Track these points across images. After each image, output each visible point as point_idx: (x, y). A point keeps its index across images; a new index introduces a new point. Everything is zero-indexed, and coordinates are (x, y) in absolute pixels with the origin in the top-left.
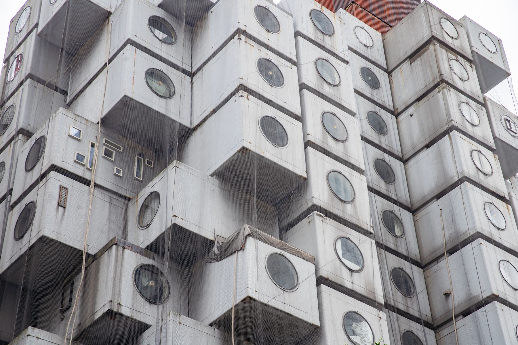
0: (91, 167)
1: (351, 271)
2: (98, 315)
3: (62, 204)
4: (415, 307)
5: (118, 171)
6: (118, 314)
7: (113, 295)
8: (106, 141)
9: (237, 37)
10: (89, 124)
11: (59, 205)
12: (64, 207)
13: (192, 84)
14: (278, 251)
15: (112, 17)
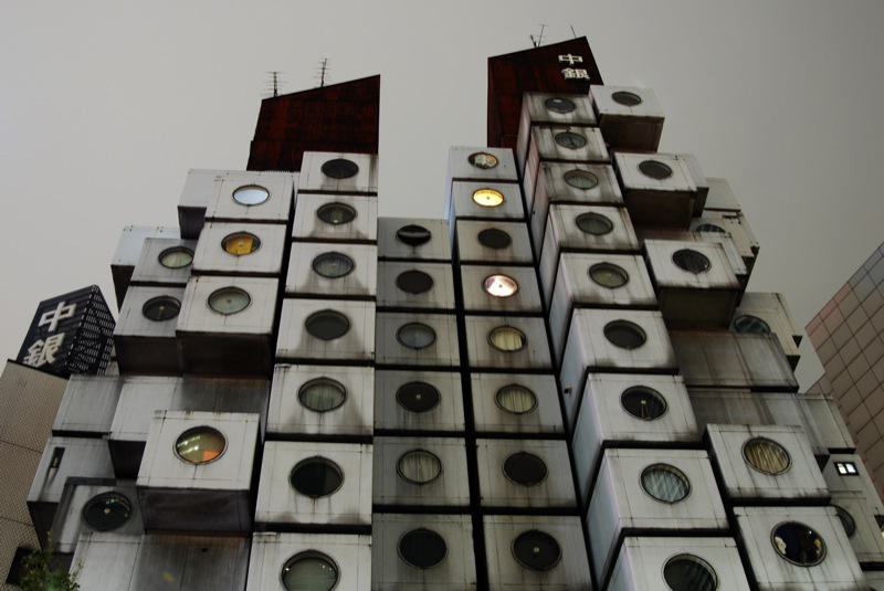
11: (51, 466)
12: (57, 467)
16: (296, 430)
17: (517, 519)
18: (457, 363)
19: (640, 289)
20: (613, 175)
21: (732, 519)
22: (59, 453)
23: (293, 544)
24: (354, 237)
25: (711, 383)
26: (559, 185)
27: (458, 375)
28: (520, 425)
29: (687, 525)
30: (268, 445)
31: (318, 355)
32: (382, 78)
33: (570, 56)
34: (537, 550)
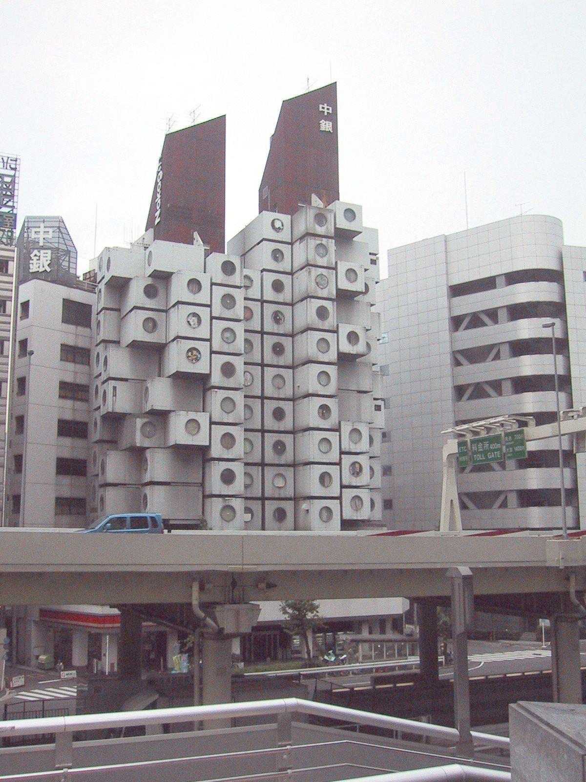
3: (115, 395)
11: (113, 396)
12: (115, 396)
19: (332, 356)
21: (341, 459)
22: (115, 388)
23: (224, 466)
24: (235, 317)
26: (313, 284)
27: (260, 367)
29: (328, 461)
32: (227, 117)
33: (325, 106)
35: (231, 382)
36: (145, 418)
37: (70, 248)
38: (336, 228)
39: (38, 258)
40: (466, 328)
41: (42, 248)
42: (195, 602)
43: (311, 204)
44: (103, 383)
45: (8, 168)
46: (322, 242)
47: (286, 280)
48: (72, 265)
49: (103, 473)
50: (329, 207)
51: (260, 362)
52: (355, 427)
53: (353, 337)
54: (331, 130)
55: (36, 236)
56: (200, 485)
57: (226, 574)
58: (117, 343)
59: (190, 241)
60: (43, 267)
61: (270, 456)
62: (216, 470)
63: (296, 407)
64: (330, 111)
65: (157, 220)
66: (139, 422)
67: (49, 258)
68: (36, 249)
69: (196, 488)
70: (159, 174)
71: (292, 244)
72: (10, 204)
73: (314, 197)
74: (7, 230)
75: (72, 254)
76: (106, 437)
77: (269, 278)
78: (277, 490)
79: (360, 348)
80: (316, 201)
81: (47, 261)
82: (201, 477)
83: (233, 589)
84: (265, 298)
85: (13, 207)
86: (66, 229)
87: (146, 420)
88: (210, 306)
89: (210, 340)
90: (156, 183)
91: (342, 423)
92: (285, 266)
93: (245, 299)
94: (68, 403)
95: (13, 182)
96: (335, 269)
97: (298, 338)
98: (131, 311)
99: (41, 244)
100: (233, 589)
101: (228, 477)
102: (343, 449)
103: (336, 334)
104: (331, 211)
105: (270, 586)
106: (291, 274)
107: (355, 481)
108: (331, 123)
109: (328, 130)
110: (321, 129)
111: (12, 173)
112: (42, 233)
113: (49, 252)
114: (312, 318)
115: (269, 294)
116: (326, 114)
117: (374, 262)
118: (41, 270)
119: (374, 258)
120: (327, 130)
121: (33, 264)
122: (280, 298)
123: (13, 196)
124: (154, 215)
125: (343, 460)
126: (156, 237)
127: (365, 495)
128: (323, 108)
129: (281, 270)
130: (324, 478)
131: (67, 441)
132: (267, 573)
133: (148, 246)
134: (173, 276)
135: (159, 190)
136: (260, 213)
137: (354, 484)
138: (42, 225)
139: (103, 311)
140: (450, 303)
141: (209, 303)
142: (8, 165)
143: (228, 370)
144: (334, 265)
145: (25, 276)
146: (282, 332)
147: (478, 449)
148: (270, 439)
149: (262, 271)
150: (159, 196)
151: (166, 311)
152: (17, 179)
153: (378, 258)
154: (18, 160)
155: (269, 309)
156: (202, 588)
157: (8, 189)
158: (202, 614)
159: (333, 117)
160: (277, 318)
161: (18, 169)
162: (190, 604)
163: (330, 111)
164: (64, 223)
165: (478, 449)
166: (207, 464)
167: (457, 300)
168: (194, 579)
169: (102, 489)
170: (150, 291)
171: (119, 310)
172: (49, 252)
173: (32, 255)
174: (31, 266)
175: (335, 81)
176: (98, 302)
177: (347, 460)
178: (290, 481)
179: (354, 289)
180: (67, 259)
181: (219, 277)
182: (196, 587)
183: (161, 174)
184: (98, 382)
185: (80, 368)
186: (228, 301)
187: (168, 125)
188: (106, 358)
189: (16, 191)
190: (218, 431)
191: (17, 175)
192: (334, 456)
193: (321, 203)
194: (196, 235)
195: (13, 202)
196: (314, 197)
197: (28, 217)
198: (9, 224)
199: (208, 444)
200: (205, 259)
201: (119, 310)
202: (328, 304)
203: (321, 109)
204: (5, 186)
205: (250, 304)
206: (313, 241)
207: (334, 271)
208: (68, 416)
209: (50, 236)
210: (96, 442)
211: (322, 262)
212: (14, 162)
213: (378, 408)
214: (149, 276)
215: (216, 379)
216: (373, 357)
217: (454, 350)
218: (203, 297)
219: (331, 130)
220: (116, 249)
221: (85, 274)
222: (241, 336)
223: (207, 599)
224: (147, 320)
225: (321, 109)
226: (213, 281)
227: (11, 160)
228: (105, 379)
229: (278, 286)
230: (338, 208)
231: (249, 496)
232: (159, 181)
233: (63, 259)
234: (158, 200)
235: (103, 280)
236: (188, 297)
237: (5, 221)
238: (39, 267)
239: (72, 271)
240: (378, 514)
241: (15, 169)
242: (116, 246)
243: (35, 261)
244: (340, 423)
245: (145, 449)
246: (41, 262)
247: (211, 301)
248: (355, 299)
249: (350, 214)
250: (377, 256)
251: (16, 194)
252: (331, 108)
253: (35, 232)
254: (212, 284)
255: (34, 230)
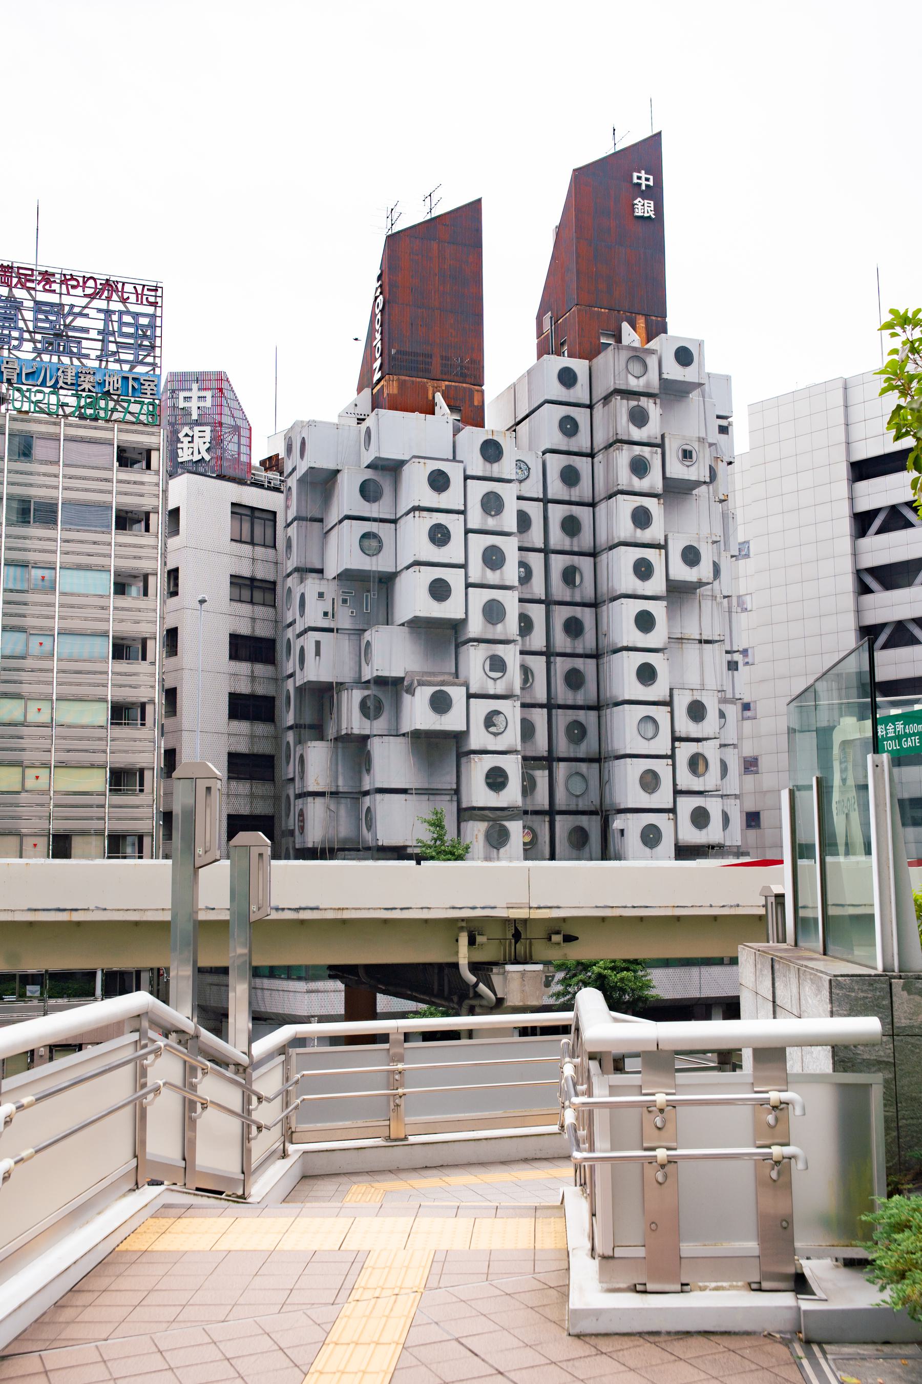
0: (333, 617)
1: (495, 680)
2: (343, 733)
3: (318, 653)
4: (581, 646)
5: (352, 612)
6: (352, 734)
7: (347, 725)
8: (343, 592)
9: (412, 515)
10: (330, 582)
11: (316, 655)
13: (396, 530)
14: (438, 688)
15: (339, 476)
16: (484, 692)
17: (570, 712)
18: (543, 598)
19: (656, 585)
20: (659, 456)
21: (673, 749)
22: (318, 644)
23: (489, 762)
25: (679, 636)
28: (574, 648)
30: (472, 700)
31: (489, 636)
33: (643, 174)
34: (576, 732)
35: (498, 631)
36: (367, 688)
37: (239, 423)
38: (660, 379)
39: (190, 439)
40: (880, 531)
41: (197, 423)
42: (463, 962)
43: (619, 340)
44: (300, 635)
45: (145, 302)
46: (640, 403)
47: (582, 464)
48: (244, 449)
49: (302, 778)
50: (652, 345)
51: (543, 598)
52: (695, 698)
53: (691, 556)
54: (652, 214)
55: (187, 405)
56: (453, 792)
57: (506, 921)
58: (321, 571)
59: (430, 410)
60: (199, 453)
61: (563, 747)
62: (479, 768)
63: (601, 667)
64: (651, 183)
65: (377, 376)
66: (357, 695)
67: (208, 439)
68: (186, 424)
69: (448, 798)
70: (378, 300)
71: (590, 407)
72: (149, 360)
73: (625, 326)
74: (146, 401)
75: (244, 433)
76: (308, 719)
77: (556, 463)
78: (574, 799)
79: (703, 571)
80: (631, 336)
81: (205, 443)
82: (455, 780)
83: (516, 943)
84: (550, 496)
85: (154, 365)
86: (233, 391)
87: (367, 692)
88: (463, 512)
89: (464, 566)
90: (373, 315)
91: (675, 692)
92: (582, 441)
93: (520, 498)
94: (244, 667)
95: (152, 326)
96: (662, 446)
97: (603, 557)
98: (340, 522)
99: (195, 416)
100: (516, 943)
101: (496, 780)
102: (677, 734)
103: (663, 551)
104: (652, 352)
105: (569, 939)
106: (592, 455)
107: (696, 784)
108: (652, 202)
109: (648, 215)
110: (636, 214)
111: (150, 310)
112: (195, 399)
113: (208, 429)
114: (625, 528)
115: (556, 488)
116: (643, 188)
117: (724, 430)
118: (196, 457)
119: (724, 423)
120: (646, 215)
121: (182, 449)
122: (575, 494)
123: (153, 347)
124: (372, 367)
125: (677, 750)
126: (376, 404)
127: (714, 807)
128: (639, 178)
129: (575, 449)
130: (650, 781)
131: (243, 727)
132: (564, 920)
133: (362, 417)
134: (406, 468)
135: (378, 327)
136: (538, 359)
137: (696, 788)
138: (195, 386)
139: (295, 523)
140: (851, 490)
141: (462, 508)
142: (144, 297)
143: (493, 612)
144: (659, 441)
145: (176, 468)
146: (576, 549)
147: (887, 734)
148: (563, 718)
149: (544, 453)
150: (378, 336)
151: (394, 521)
152: (158, 320)
153: (730, 424)
154: (160, 290)
155: (557, 513)
156: (472, 942)
157: (145, 336)
158: (472, 979)
159: (655, 193)
160: (571, 526)
161: (159, 304)
162: (456, 966)
163: (651, 183)
164: (229, 382)
165: (887, 734)
166: (464, 760)
167: (863, 486)
168: (461, 929)
169: (300, 801)
170: (368, 491)
171: (321, 520)
172: (208, 429)
173: (181, 435)
174: (180, 451)
175: (655, 131)
176: (287, 507)
177: (685, 751)
178: (594, 783)
179: (694, 478)
180: (236, 438)
181: (477, 466)
182: (464, 939)
183: (380, 299)
184: (290, 634)
185: (261, 611)
186: (492, 504)
187: (389, 220)
188: (303, 596)
189: (158, 340)
190: (481, 708)
191: (158, 314)
192: (662, 744)
193: (638, 338)
194: (439, 398)
195: (155, 357)
196: (625, 326)
197: (172, 374)
198: (149, 393)
199: (465, 729)
200: (454, 435)
201: (321, 520)
202: (651, 504)
203: (635, 180)
204: (140, 332)
205: (527, 506)
206: (625, 402)
207: (659, 450)
208: (244, 688)
209: (208, 403)
210: (290, 728)
211: (637, 434)
212: (153, 293)
213: (733, 666)
214: (368, 467)
215: (476, 626)
216: (724, 585)
217: (858, 568)
218: (451, 498)
219: (652, 214)
220: (311, 424)
221: (263, 463)
222: (512, 556)
223: (482, 956)
224: (366, 536)
225: (635, 180)
226: (469, 473)
227: (148, 290)
228: (302, 629)
229: (570, 476)
230: (664, 346)
231: (530, 808)
232: (377, 311)
233: (229, 439)
234: (377, 343)
235: (294, 474)
236: (430, 498)
237: (143, 387)
238: (192, 454)
239: (244, 458)
240: (735, 835)
241: (154, 304)
242: (312, 419)
243: (185, 445)
244: (671, 690)
245: (365, 738)
246: (195, 445)
247: (465, 505)
248: (694, 492)
249: (684, 356)
250: (730, 420)
251: (158, 343)
252: (651, 177)
253: (185, 398)
254: (466, 478)
255: (182, 395)
